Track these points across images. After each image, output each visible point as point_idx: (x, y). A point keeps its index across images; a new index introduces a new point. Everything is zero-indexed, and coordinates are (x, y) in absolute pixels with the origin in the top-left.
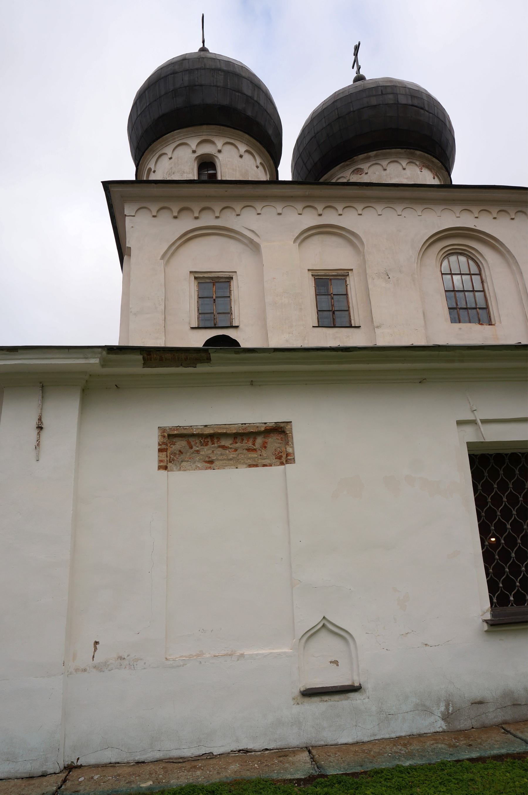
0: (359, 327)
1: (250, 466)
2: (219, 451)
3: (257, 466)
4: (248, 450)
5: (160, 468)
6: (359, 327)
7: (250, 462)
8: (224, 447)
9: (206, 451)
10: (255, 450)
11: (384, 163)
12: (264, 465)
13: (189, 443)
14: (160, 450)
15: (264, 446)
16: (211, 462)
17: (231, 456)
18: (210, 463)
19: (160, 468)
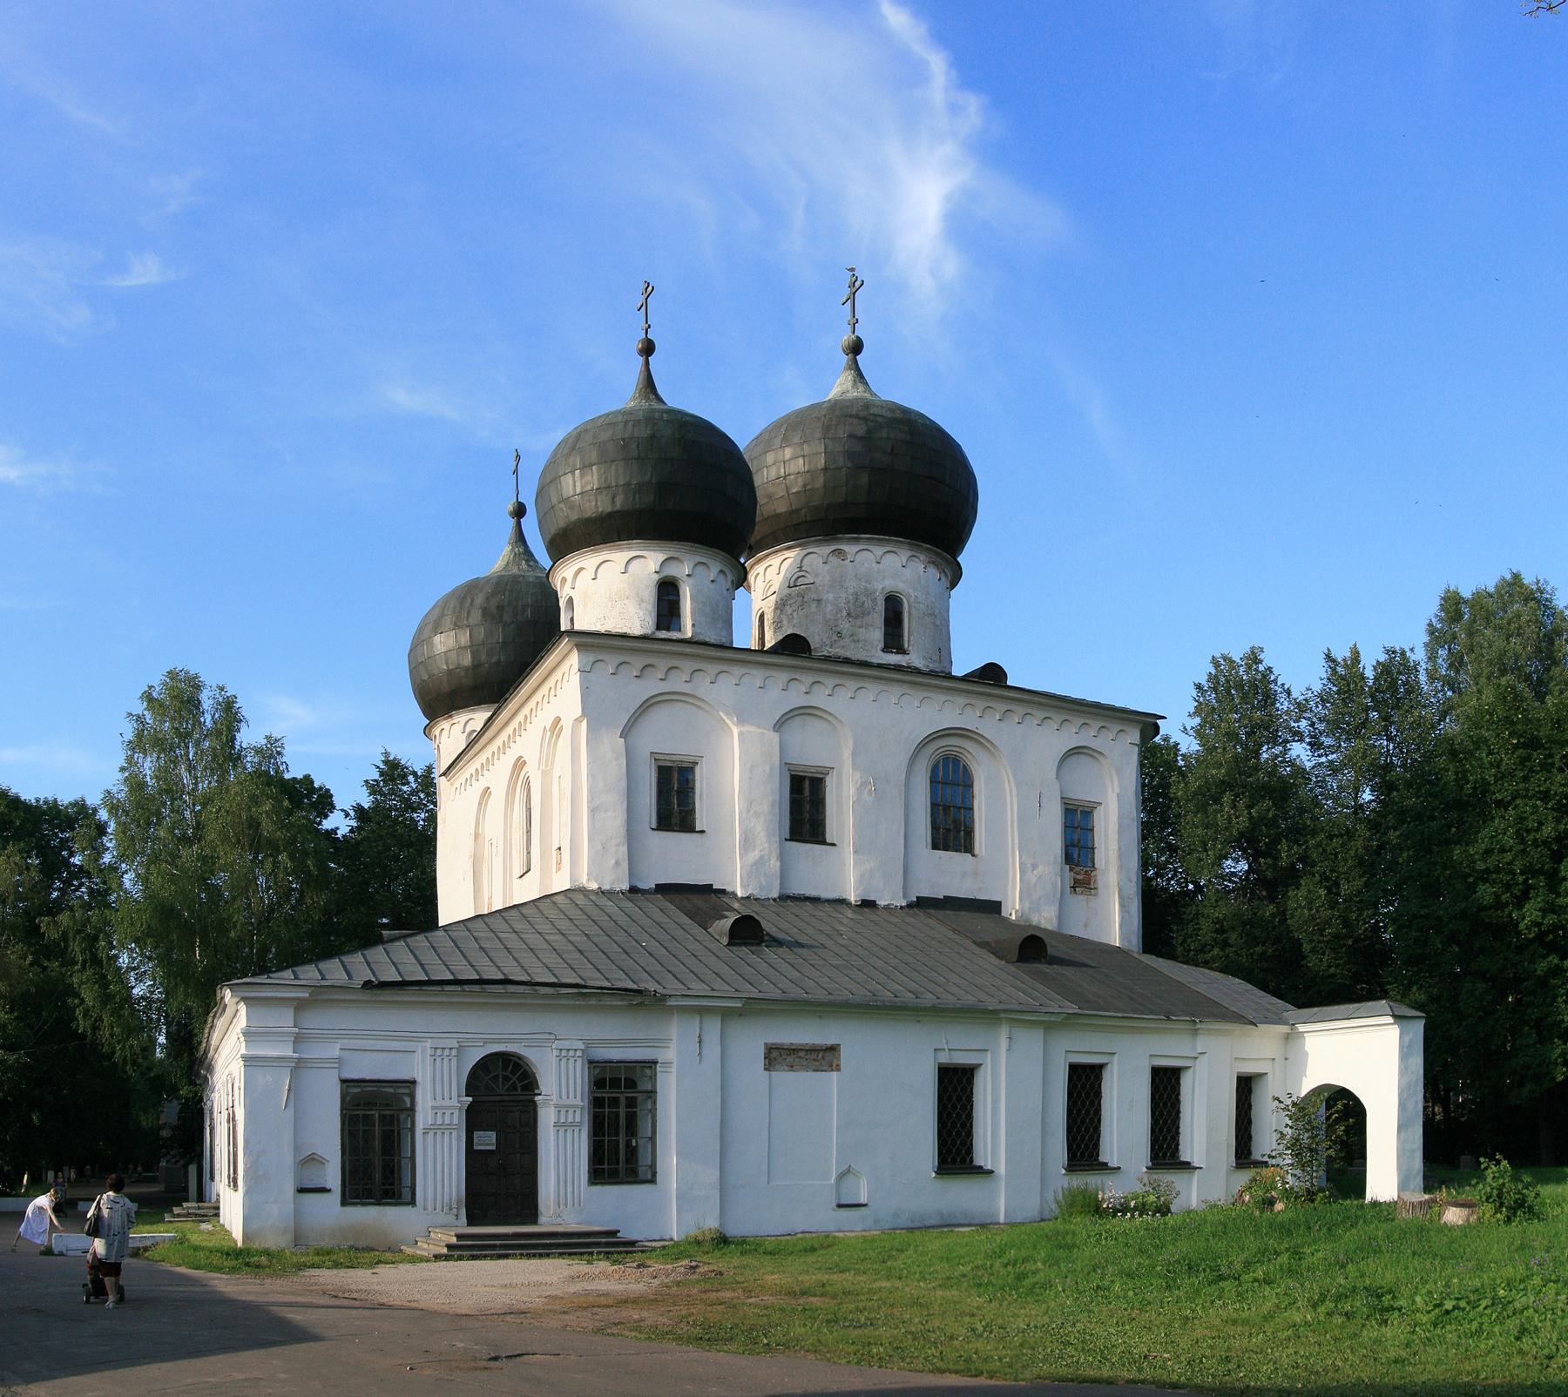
0: (834, 845)
1: (814, 1071)
2: (797, 1060)
3: (817, 1071)
4: (815, 1060)
5: (765, 1069)
6: (834, 845)
7: (814, 1068)
8: (800, 1057)
9: (790, 1059)
10: (818, 1061)
11: (879, 550)
12: (822, 1071)
13: (780, 1053)
14: (765, 1058)
15: (823, 1058)
16: (792, 1067)
17: (804, 1063)
18: (792, 1068)
19: (765, 1069)
